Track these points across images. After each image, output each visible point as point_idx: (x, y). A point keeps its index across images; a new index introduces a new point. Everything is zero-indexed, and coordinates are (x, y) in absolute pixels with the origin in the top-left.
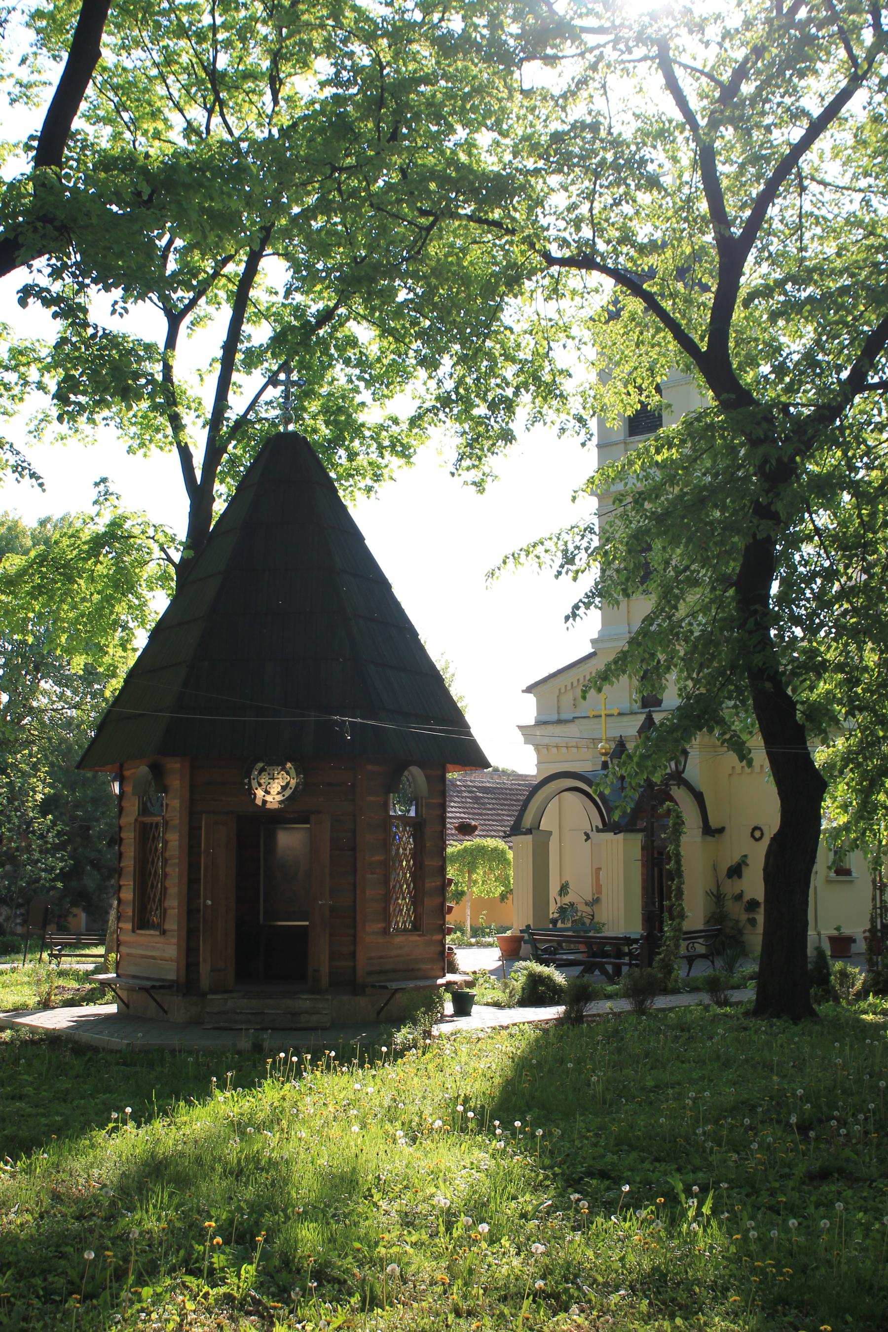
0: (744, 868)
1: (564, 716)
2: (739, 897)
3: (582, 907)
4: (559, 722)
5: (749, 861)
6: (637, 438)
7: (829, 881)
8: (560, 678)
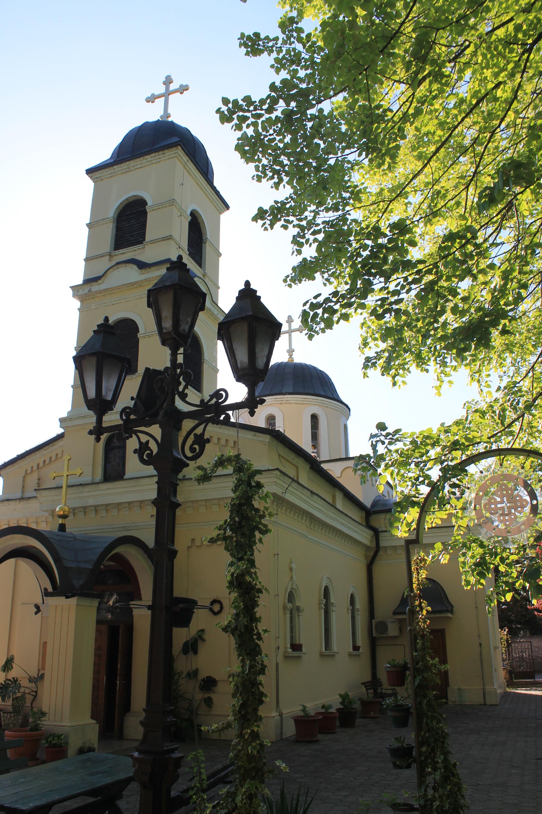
0: (200, 643)
1: (27, 495)
3: (24, 683)
4: (22, 499)
5: (205, 637)
6: (121, 251)
7: (287, 657)
8: (28, 459)
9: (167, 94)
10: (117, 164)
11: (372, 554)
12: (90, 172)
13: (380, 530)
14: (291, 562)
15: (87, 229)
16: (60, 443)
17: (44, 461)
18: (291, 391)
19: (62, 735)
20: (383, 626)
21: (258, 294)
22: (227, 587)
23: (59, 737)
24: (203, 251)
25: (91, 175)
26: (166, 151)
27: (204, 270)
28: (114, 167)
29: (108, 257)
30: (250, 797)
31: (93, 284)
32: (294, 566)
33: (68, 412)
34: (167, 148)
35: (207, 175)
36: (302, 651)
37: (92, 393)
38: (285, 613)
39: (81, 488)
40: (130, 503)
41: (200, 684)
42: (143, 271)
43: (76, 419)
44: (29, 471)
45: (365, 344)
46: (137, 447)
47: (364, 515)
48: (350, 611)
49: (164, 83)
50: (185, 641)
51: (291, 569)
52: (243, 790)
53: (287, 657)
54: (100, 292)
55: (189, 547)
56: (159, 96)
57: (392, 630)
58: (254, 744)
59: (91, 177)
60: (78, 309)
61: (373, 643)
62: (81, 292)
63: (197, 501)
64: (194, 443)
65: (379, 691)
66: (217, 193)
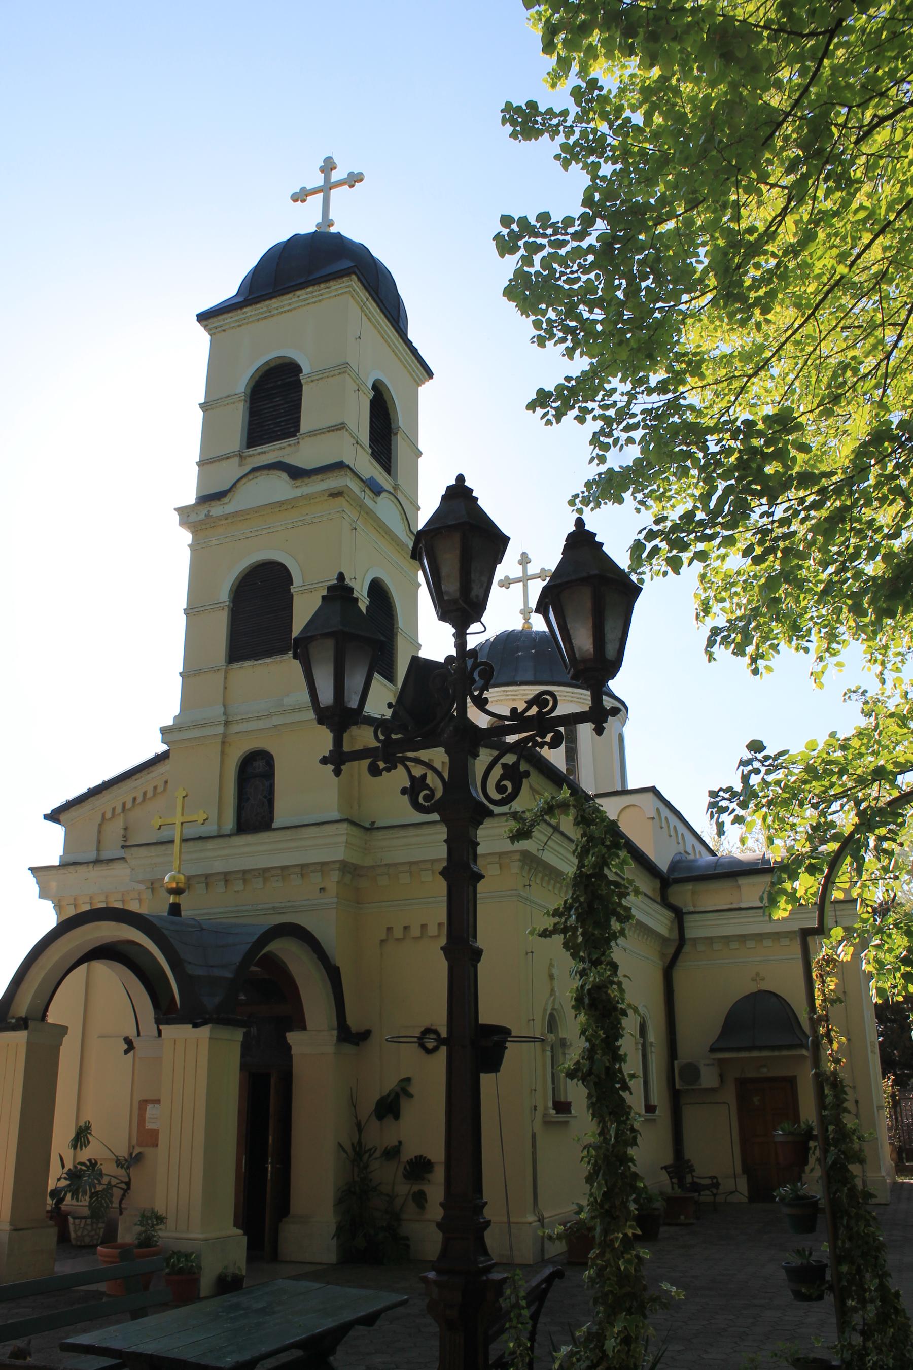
1: (106, 855)
2: (393, 1153)
3: (109, 1168)
4: (97, 862)
5: (412, 1090)
6: (259, 449)
7: (548, 1123)
8: (107, 796)
9: (326, 188)
10: (250, 305)
11: (671, 951)
12: (203, 317)
13: (684, 910)
14: (551, 965)
15: (200, 413)
16: (162, 768)
17: (135, 799)
18: (531, 678)
19: (192, 1254)
20: (692, 1072)
21: (598, 539)
22: (573, 1007)
23: (187, 1256)
24: (393, 447)
25: (205, 323)
26: (331, 283)
27: (395, 479)
28: (245, 310)
29: (237, 459)
30: (627, 1340)
31: (213, 503)
32: (555, 971)
33: (175, 718)
34: (334, 279)
35: (397, 322)
36: (570, 1113)
37: (326, 696)
38: (544, 1051)
39: (200, 845)
40: (284, 868)
41: (405, 1168)
42: (298, 482)
43: (188, 728)
44: (108, 816)
45: (706, 609)
46: (408, 785)
47: (659, 886)
48: (640, 1047)
49: (322, 170)
50: (378, 1097)
51: (551, 977)
52: (616, 1330)
53: (548, 1123)
54: (226, 517)
55: (382, 941)
56: (314, 192)
57: (708, 1078)
58: (627, 1256)
59: (205, 327)
60: (189, 546)
61: (676, 1098)
62: (193, 518)
63: (395, 865)
64: (503, 778)
65: (689, 1179)
66: (414, 351)
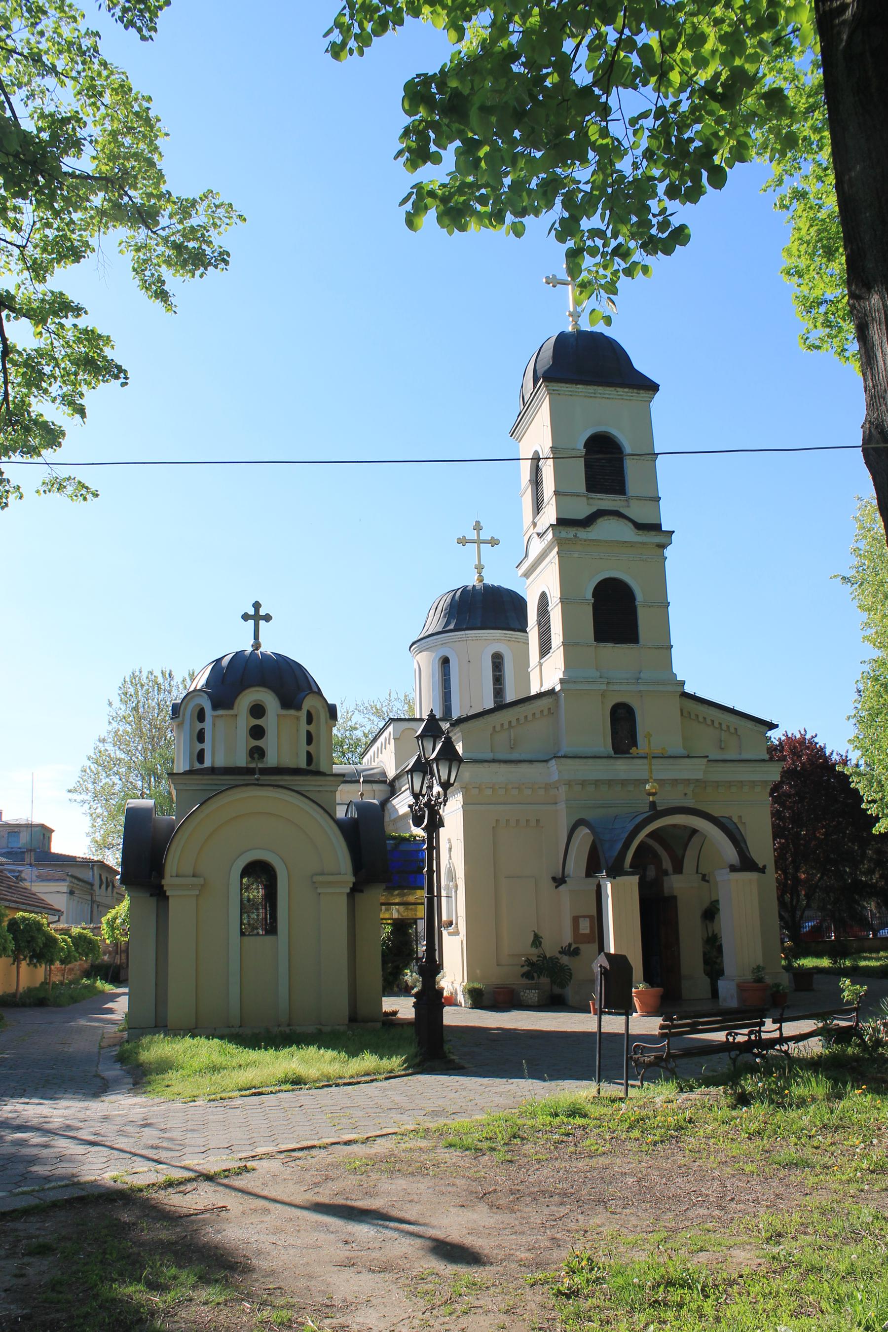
42: (640, 532)
43: (575, 682)
